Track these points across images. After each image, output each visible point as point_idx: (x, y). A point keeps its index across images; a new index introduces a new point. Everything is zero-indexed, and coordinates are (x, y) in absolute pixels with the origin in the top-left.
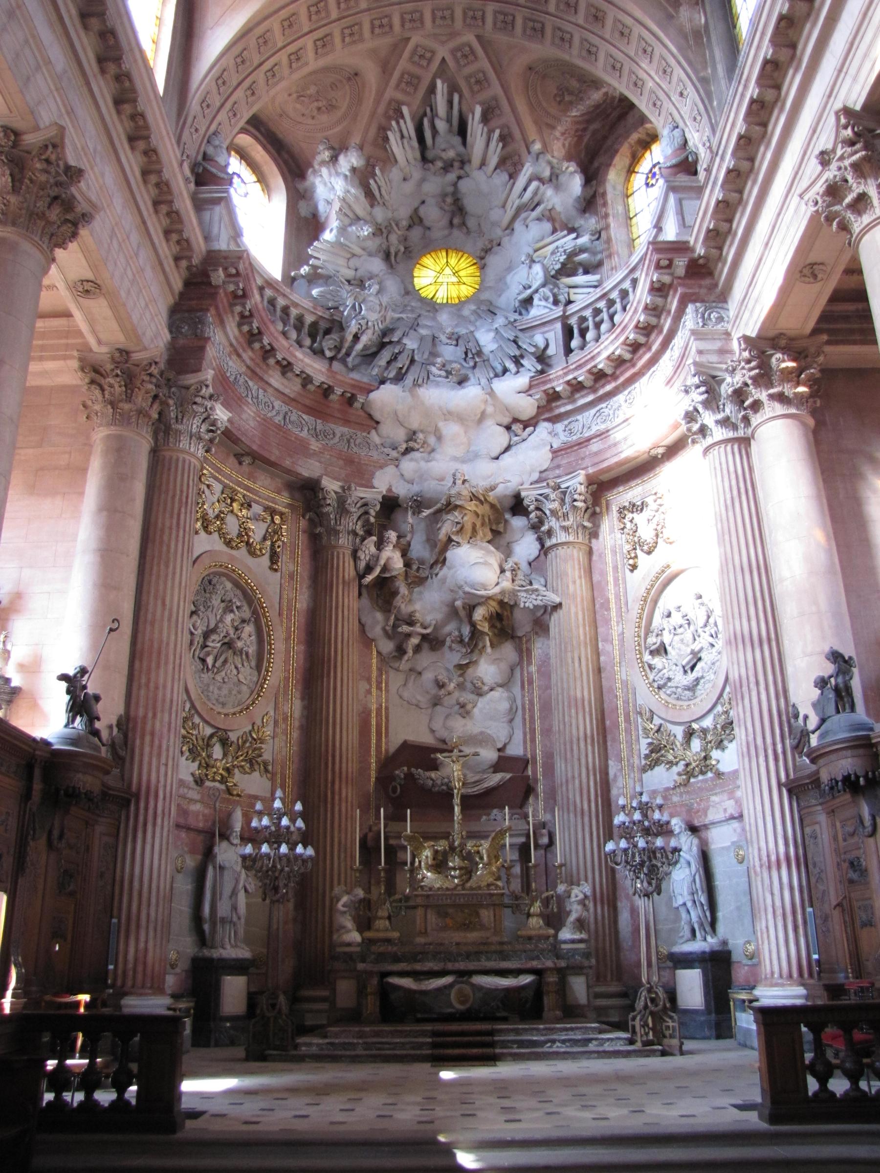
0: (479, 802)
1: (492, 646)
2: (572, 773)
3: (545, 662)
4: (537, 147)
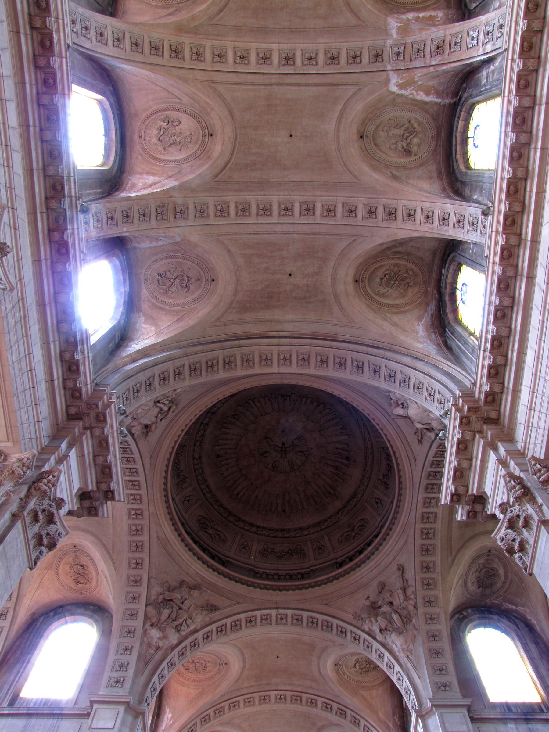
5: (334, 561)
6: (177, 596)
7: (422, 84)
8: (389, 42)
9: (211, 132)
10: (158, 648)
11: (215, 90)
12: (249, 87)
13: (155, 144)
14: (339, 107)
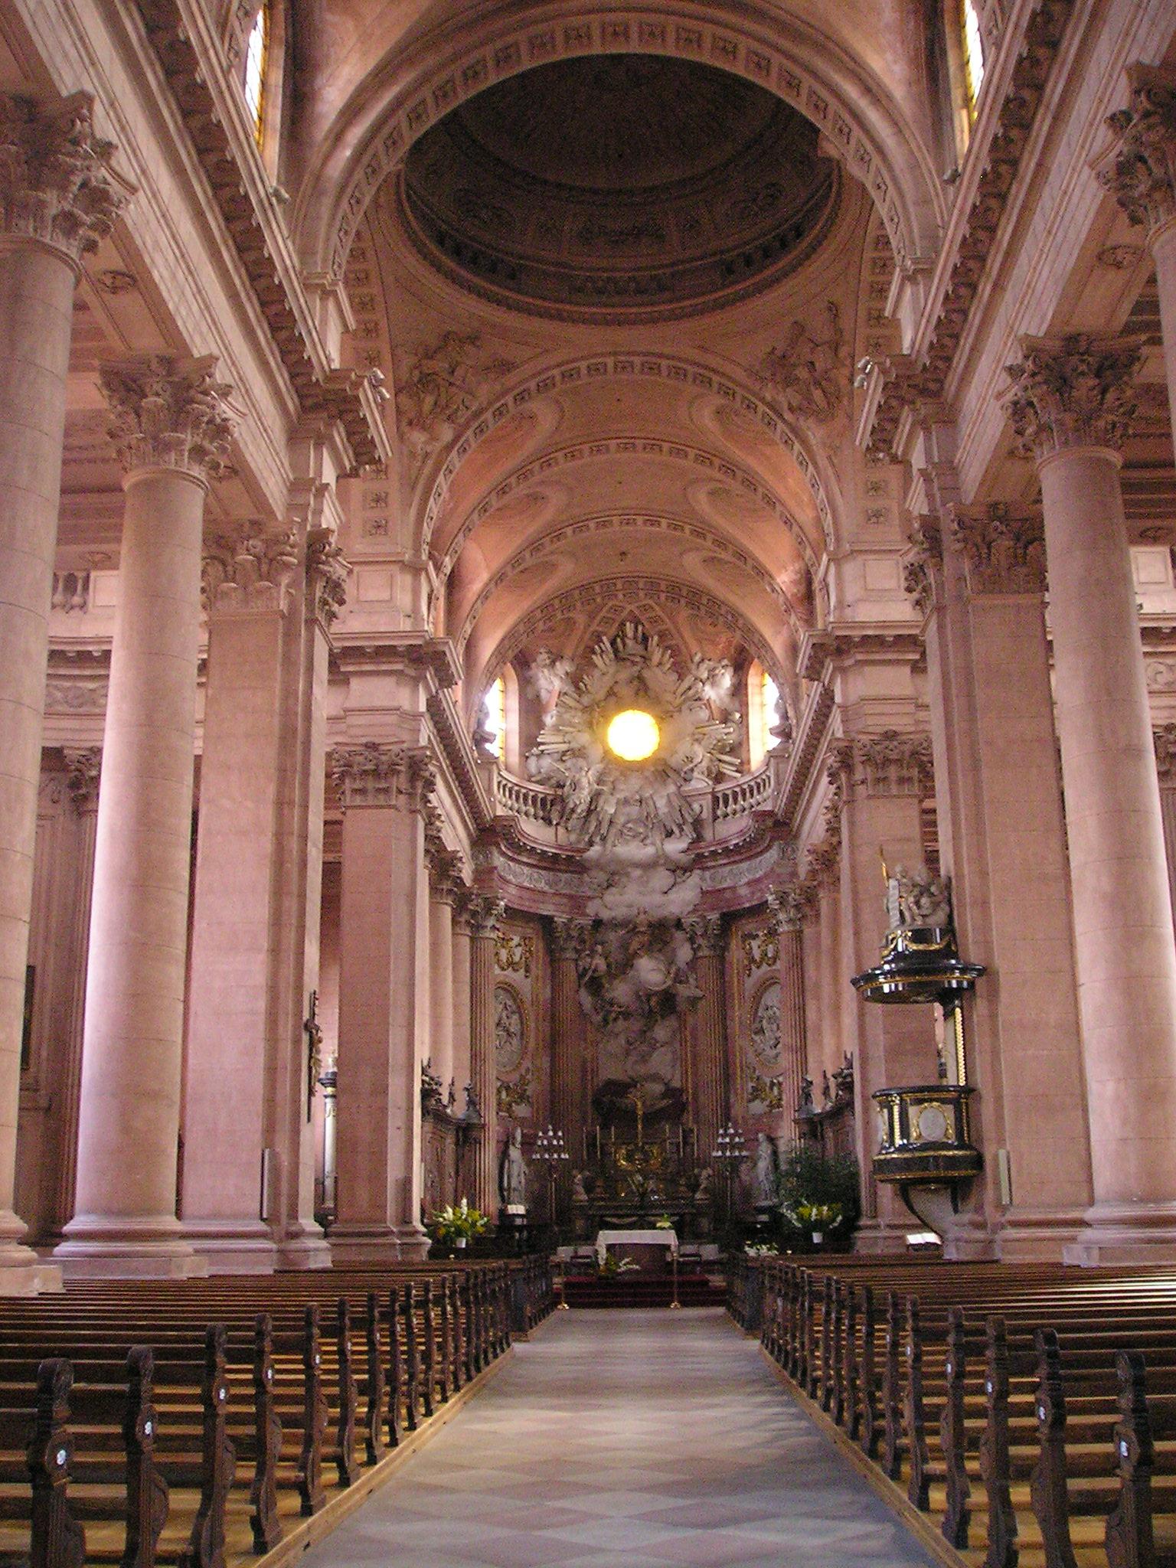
0: (653, 1118)
1: (663, 1017)
2: (708, 1101)
3: (694, 1029)
4: (697, 659)
5: (718, 258)
6: (440, 365)
10: (427, 455)
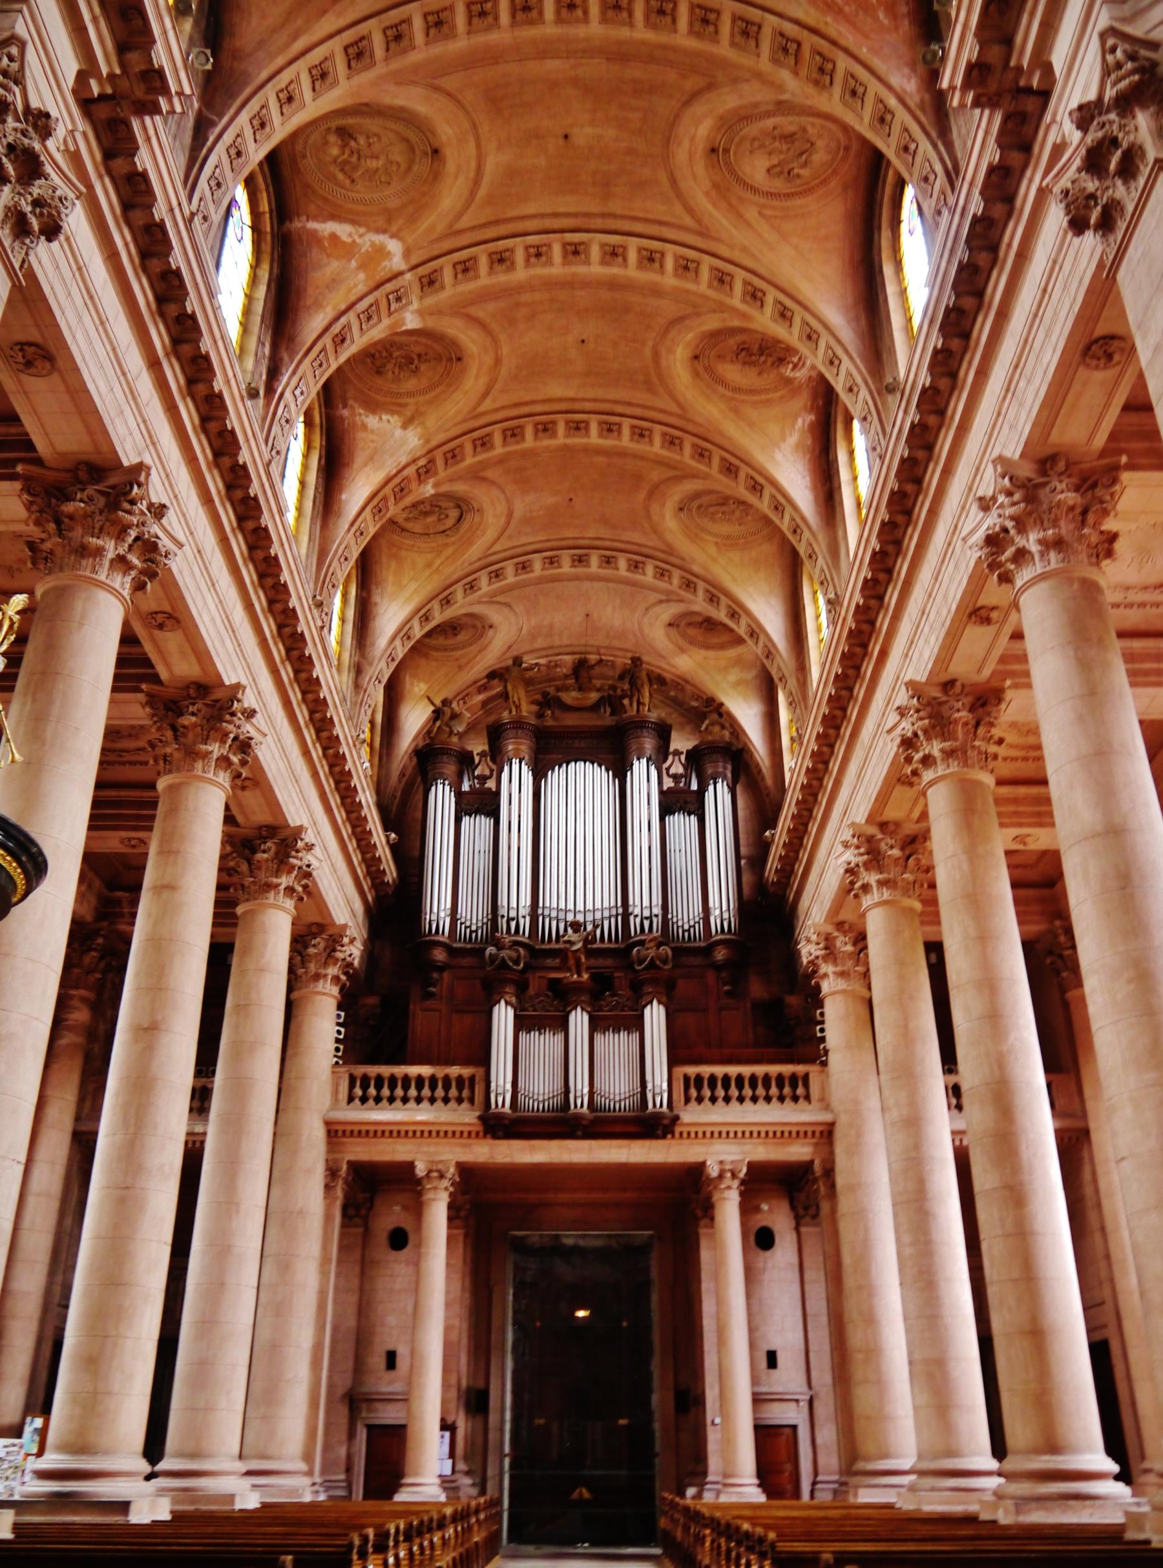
7: (349, 261)
8: (415, 305)
9: (714, 156)
11: (699, 221)
12: (640, 215)
13: (820, 136)
14: (482, 192)
